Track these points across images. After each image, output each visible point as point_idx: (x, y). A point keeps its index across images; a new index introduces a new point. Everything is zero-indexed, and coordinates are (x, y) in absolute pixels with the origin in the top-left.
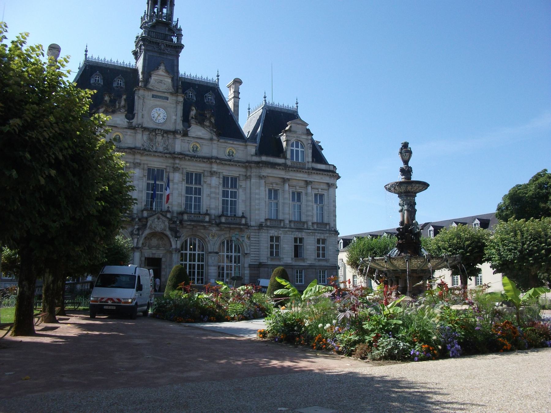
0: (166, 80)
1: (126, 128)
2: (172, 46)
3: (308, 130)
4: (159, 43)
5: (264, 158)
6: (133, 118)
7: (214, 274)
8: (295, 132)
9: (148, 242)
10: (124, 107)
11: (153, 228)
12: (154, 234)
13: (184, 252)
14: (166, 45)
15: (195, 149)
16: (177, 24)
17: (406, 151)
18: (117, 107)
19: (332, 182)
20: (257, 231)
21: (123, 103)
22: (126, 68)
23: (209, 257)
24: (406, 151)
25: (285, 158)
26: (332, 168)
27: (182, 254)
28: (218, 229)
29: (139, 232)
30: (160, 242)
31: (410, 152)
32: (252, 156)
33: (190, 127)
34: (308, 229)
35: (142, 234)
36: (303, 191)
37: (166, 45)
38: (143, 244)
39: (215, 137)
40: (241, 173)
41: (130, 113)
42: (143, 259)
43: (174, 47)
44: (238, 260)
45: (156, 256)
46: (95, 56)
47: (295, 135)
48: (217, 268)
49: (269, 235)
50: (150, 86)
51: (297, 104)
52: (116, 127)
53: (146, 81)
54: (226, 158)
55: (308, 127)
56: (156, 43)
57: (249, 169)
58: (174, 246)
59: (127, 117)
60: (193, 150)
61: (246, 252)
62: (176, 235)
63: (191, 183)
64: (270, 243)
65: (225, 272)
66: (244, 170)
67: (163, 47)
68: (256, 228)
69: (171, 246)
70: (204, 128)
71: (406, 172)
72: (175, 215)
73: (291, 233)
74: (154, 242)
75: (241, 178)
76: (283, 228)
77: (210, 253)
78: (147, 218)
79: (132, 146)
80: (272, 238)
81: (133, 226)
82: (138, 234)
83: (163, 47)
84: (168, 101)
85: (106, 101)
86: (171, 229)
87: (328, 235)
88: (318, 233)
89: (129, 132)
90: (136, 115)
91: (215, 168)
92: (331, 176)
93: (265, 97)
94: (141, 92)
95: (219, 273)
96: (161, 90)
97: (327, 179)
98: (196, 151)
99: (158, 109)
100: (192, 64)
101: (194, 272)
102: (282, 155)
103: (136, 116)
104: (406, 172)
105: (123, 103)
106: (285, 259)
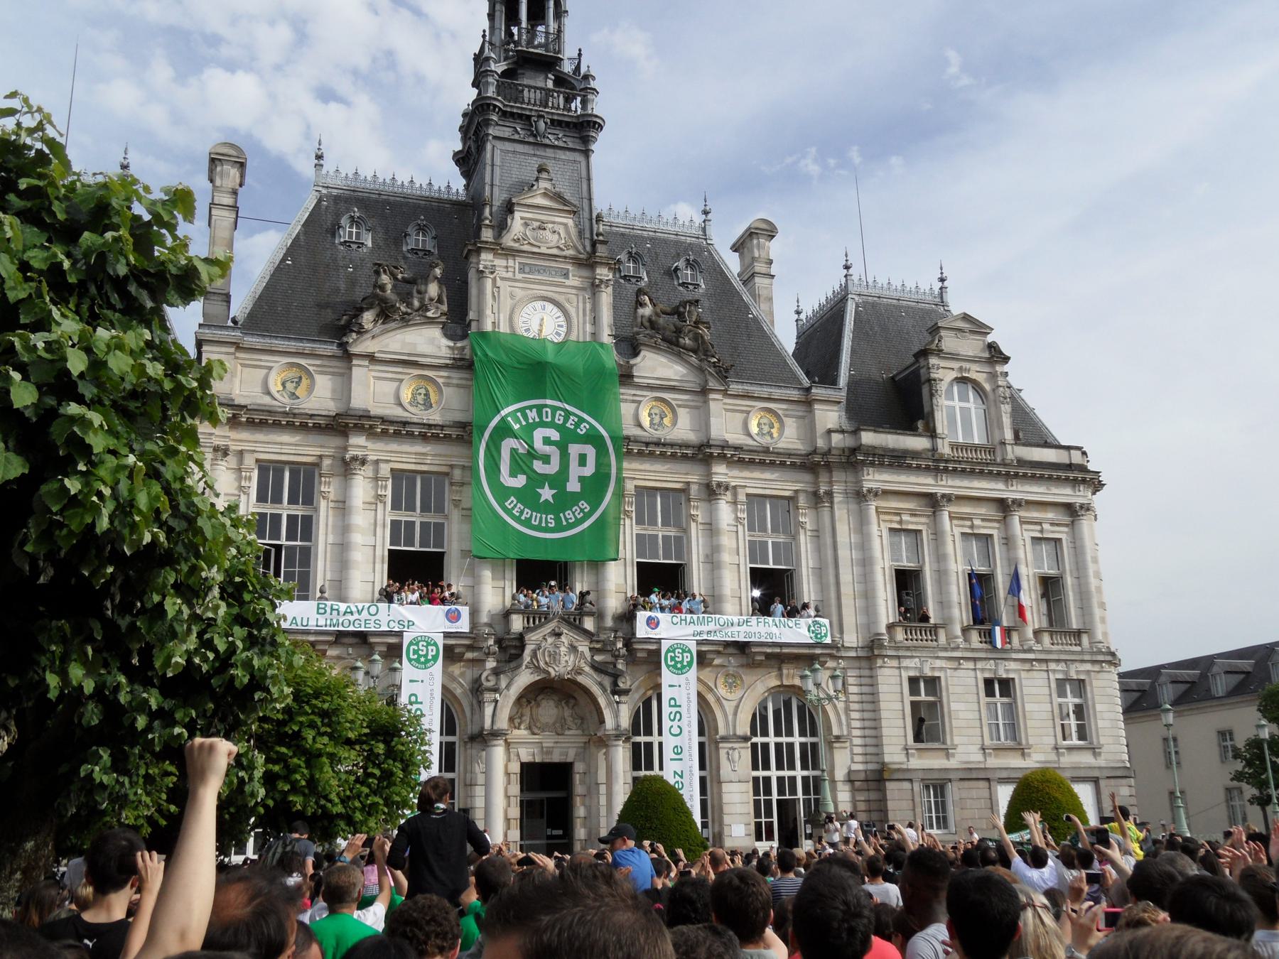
0: (557, 219)
1: (446, 367)
2: (568, 124)
3: (992, 347)
4: (529, 117)
5: (868, 438)
7: (739, 809)
8: (954, 357)
9: (527, 711)
10: (440, 301)
11: (542, 664)
12: (544, 689)
13: (642, 739)
14: (552, 121)
15: (657, 420)
16: (578, 68)
19: (1084, 501)
20: (864, 664)
21: (433, 290)
22: (439, 200)
23: (723, 753)
25: (932, 433)
26: (1076, 458)
27: (636, 747)
28: (744, 660)
29: (498, 680)
30: (567, 713)
32: (830, 432)
33: (636, 354)
34: (1025, 651)
35: (508, 687)
36: (995, 532)
37: (552, 121)
38: (511, 719)
39: (712, 384)
40: (798, 486)
42: (515, 768)
43: (575, 125)
44: (811, 756)
45: (556, 758)
46: (347, 170)
47: (956, 365)
48: (750, 786)
49: (905, 675)
50: (508, 241)
51: (942, 280)
53: (501, 227)
54: (751, 442)
55: (990, 339)
56: (520, 116)
57: (824, 477)
58: (609, 723)
60: (652, 423)
61: (836, 732)
62: (615, 684)
63: (653, 522)
64: (908, 699)
65: (775, 796)
66: (808, 477)
67: (542, 125)
68: (861, 654)
69: (602, 721)
70: (679, 355)
72: (609, 622)
73: (970, 665)
74: (548, 710)
75: (802, 501)
76: (945, 649)
77: (725, 739)
78: (521, 638)
80: (913, 681)
81: (479, 662)
82: (495, 690)
83: (542, 125)
84: (568, 282)
86: (596, 667)
87: (1088, 667)
88: (1058, 661)
91: (721, 472)
92: (1075, 483)
93: (847, 267)
94: (486, 258)
95: (757, 803)
96: (544, 250)
97: (1063, 494)
98: (661, 424)
99: (539, 304)
100: (629, 178)
102: (920, 424)
106: (960, 749)
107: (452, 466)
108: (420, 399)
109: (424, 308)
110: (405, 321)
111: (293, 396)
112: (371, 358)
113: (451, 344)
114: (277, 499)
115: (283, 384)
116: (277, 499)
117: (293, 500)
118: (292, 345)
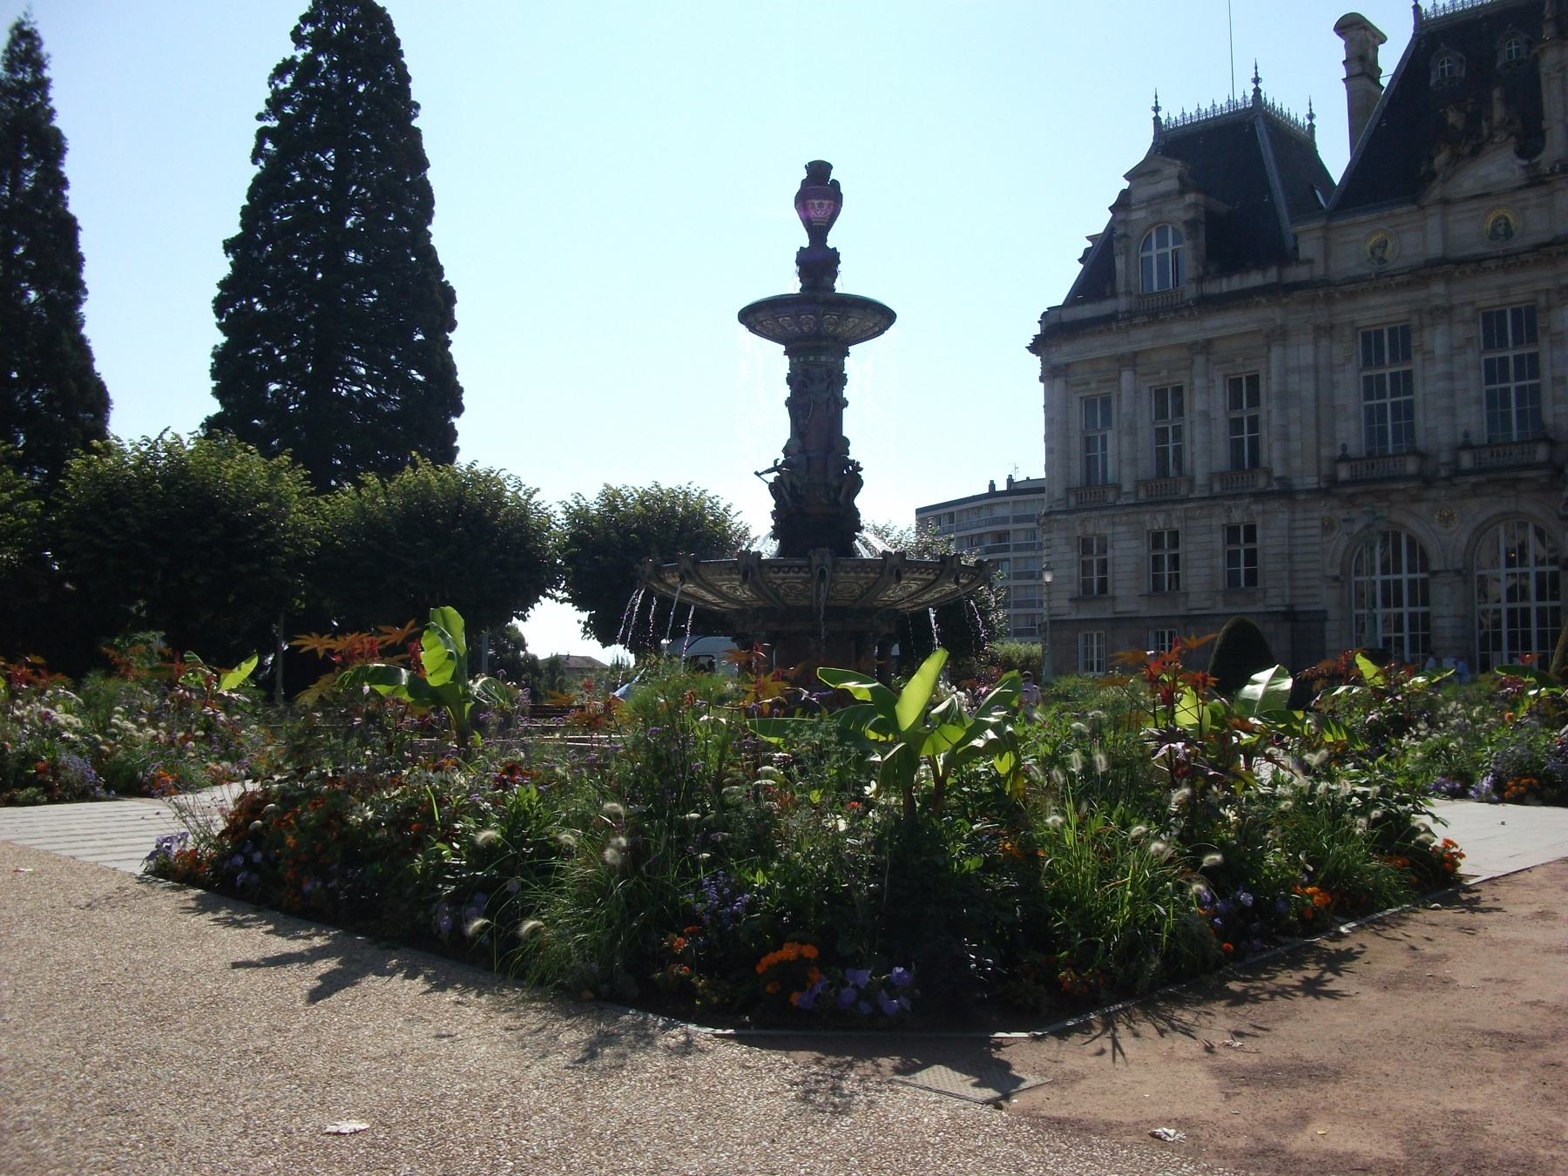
6: (1539, 150)
10: (1511, 122)
17: (819, 193)
18: (1485, 132)
21: (1498, 113)
24: (819, 193)
31: (802, 200)
41: (1529, 140)
52: (1488, 195)
59: (1520, 153)
71: (818, 263)
79: (1546, 238)
85: (1453, 126)
89: (1532, 195)
90: (1548, 134)
101: (1527, 635)
103: (1548, 141)
104: (818, 263)
105: (1498, 113)
107: (1537, 292)
108: (1501, 230)
109: (1491, 135)
110: (1476, 152)
111: (1382, 260)
112: (1446, 202)
113: (1525, 163)
114: (1380, 363)
115: (1373, 253)
116: (1380, 363)
117: (1394, 359)
118: (1374, 216)
